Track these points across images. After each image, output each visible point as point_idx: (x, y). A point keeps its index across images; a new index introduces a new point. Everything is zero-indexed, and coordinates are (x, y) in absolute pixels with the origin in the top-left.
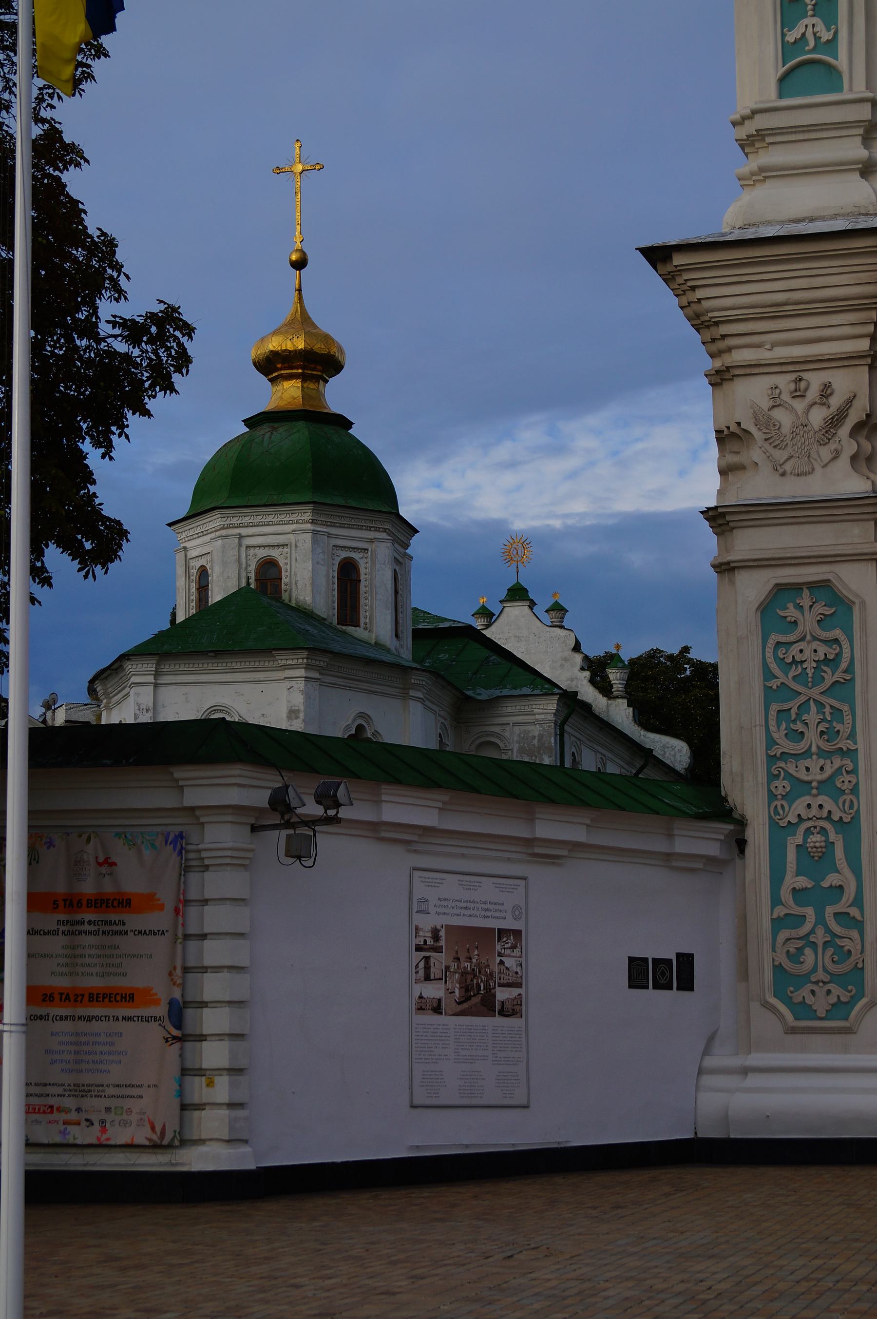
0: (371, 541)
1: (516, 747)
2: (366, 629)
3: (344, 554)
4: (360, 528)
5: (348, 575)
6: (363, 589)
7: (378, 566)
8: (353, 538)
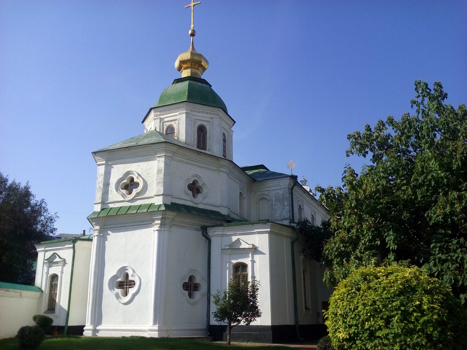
0: (212, 118)
1: (274, 199)
2: (209, 151)
3: (200, 123)
4: (207, 113)
5: (202, 130)
7: (214, 128)
8: (203, 117)
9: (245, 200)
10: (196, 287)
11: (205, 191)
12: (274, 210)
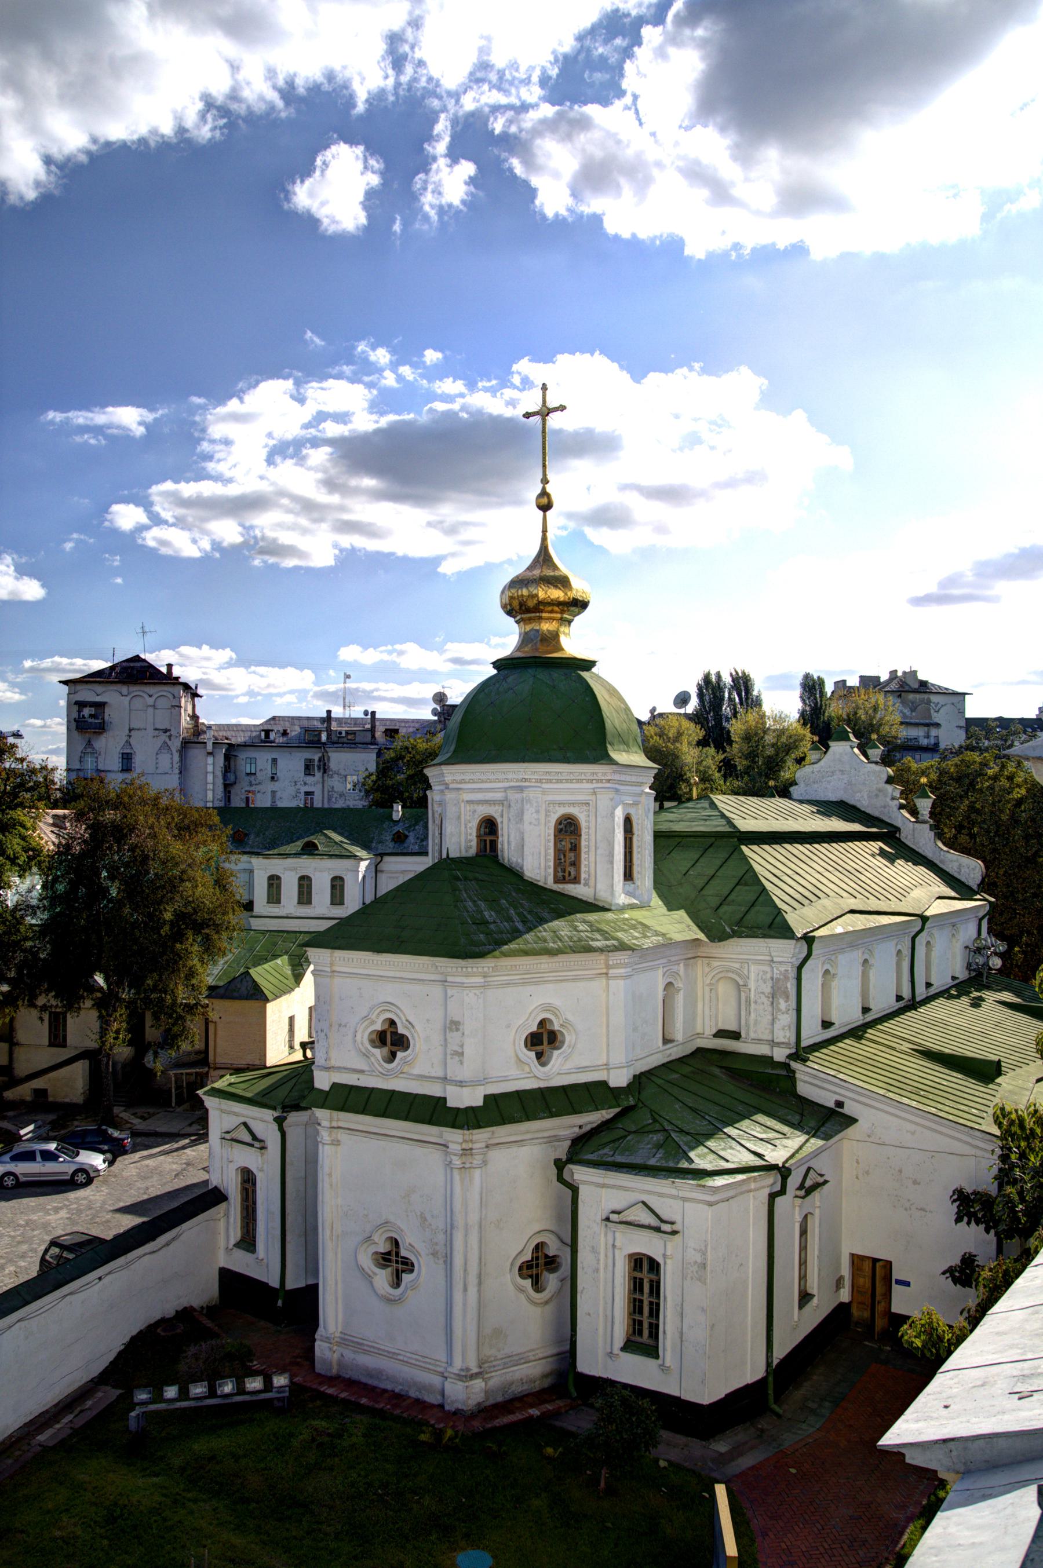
3: (561, 811)
5: (568, 829)
6: (583, 843)
9: (682, 992)
10: (551, 1263)
11: (568, 1039)
12: (753, 1015)
